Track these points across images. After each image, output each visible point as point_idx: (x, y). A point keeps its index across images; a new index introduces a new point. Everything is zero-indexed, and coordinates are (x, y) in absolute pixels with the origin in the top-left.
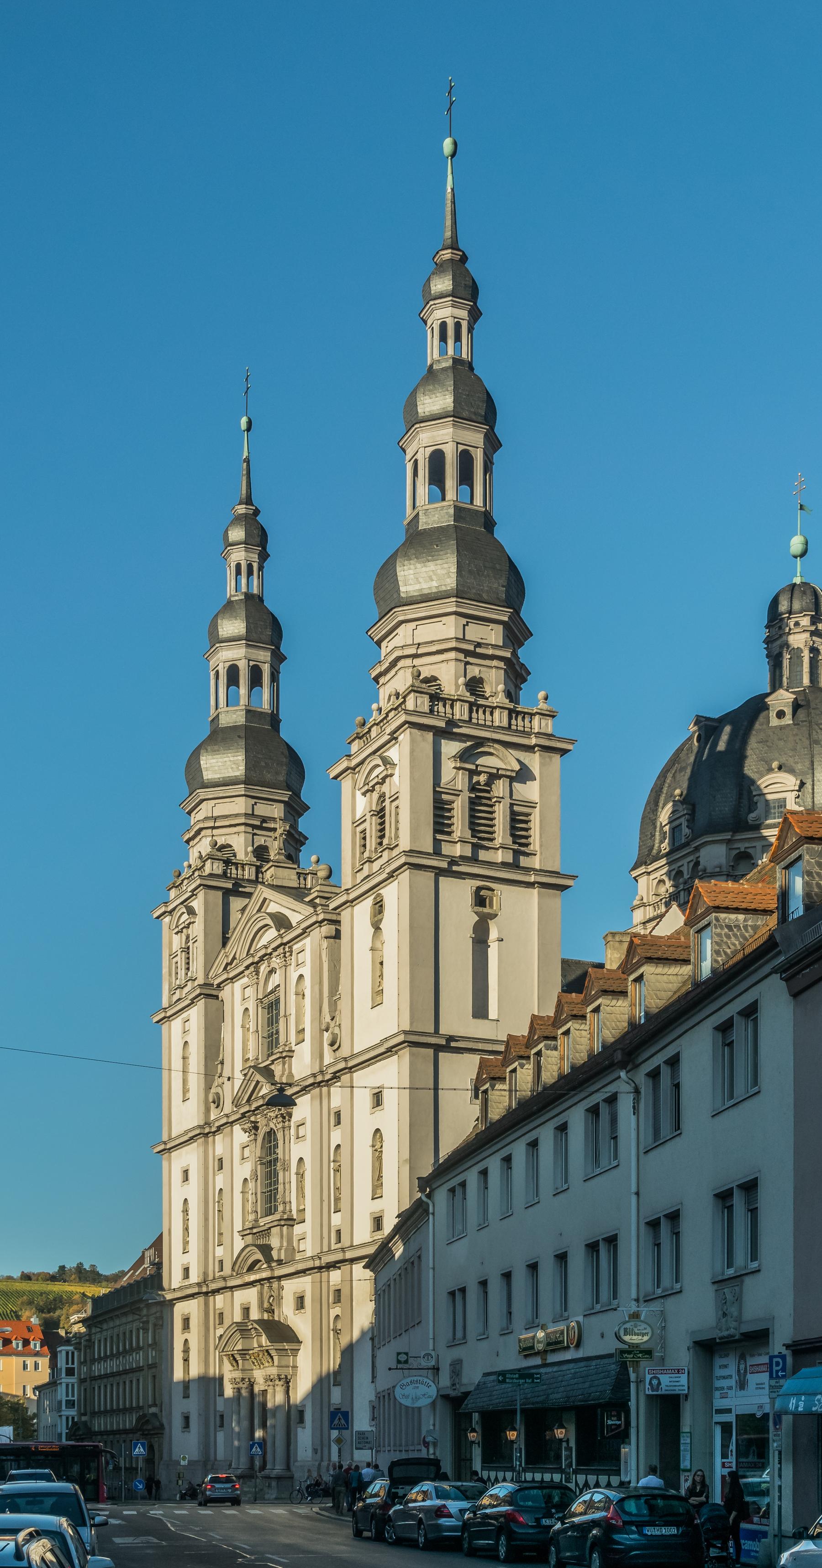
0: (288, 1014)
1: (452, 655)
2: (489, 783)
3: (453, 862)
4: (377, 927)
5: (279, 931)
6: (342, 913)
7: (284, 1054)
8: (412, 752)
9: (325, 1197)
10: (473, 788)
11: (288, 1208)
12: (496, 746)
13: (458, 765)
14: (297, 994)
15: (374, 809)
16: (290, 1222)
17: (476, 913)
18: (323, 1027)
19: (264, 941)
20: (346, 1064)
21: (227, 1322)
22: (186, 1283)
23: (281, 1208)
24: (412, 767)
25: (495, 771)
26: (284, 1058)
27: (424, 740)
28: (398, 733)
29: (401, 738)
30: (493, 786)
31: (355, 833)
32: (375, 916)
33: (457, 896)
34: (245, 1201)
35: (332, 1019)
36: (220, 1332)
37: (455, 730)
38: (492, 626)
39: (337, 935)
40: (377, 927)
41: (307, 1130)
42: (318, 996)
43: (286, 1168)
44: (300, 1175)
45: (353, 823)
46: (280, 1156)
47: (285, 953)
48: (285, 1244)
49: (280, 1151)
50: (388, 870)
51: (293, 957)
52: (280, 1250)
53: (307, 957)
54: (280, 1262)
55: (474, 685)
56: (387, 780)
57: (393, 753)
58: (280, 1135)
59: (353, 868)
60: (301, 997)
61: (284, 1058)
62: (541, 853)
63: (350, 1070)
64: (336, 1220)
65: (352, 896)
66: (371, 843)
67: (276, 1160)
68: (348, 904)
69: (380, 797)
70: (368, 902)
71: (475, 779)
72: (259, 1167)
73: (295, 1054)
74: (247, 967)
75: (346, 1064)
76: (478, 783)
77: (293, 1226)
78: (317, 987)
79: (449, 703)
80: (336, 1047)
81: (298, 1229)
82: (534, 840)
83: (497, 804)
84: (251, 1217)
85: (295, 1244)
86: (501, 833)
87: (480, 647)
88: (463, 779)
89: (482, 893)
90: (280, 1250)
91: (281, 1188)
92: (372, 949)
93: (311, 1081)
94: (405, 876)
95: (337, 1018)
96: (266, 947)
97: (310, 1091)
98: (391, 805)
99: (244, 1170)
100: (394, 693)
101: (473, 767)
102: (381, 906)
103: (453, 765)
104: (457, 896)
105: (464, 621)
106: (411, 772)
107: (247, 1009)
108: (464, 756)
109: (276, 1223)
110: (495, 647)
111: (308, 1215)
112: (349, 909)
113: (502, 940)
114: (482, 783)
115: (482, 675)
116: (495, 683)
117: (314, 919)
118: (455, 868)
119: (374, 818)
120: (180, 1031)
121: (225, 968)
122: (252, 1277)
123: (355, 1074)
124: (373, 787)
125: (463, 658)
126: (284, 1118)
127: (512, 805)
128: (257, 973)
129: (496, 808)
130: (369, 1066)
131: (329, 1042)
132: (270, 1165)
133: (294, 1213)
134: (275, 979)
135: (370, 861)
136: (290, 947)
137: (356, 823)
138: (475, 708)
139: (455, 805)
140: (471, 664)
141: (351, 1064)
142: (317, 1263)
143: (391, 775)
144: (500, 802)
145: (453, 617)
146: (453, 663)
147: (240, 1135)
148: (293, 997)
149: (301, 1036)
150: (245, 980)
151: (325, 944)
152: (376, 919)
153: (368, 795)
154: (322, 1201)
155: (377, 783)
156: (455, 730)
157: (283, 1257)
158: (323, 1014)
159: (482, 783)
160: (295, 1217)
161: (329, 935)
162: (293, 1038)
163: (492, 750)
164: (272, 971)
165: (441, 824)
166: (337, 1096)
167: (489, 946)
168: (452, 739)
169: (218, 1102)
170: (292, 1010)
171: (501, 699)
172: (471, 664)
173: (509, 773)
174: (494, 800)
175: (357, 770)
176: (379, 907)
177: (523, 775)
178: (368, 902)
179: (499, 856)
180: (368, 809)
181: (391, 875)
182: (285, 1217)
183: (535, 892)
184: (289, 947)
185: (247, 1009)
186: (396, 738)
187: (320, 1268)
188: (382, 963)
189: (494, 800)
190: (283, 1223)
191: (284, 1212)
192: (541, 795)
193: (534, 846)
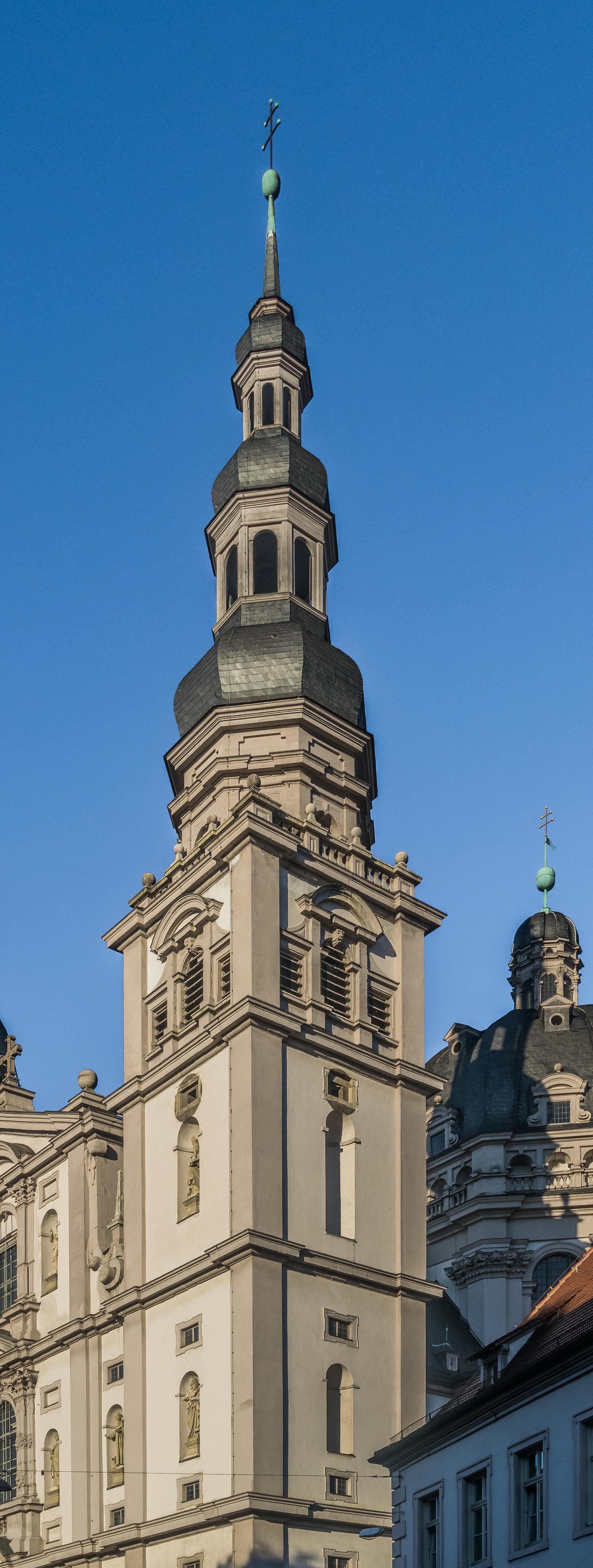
0: (29, 1261)
1: (297, 775)
2: (342, 946)
3: (306, 1028)
4: (188, 1120)
5: (19, 1157)
6: (125, 1115)
7: (26, 1307)
8: (254, 875)
10: (326, 944)
11: (31, 1492)
12: (355, 896)
13: (310, 909)
14: (43, 1236)
15: (179, 970)
16: (36, 1508)
17: (330, 1102)
18: (92, 1263)
20: (139, 1295)
23: (20, 1492)
24: (254, 895)
25: (352, 929)
26: (25, 1312)
27: (268, 865)
28: (229, 856)
29: (233, 863)
30: (347, 950)
31: (146, 1012)
32: (182, 1106)
33: (308, 1074)
35: (105, 1253)
37: (307, 862)
38: (342, 755)
39: (110, 1155)
40: (188, 1120)
42: (81, 1228)
43: (29, 1444)
44: (51, 1452)
45: (144, 999)
47: (26, 1187)
48: (29, 1534)
49: (19, 1427)
50: (214, 1033)
51: (38, 1193)
52: (22, 1540)
54: (23, 1555)
55: (324, 819)
56: (207, 928)
57: (219, 891)
58: (18, 1408)
59: (143, 1055)
60: (49, 1239)
61: (25, 1312)
62: (404, 1046)
63: (142, 1304)
65: (144, 1086)
66: (175, 1018)
67: (13, 1438)
68: (138, 1098)
69: (191, 955)
70: (172, 1091)
71: (327, 935)
73: (41, 1307)
75: (139, 1295)
76: (330, 941)
77: (39, 1512)
78: (80, 1218)
79: (295, 831)
80: (112, 1284)
82: (394, 1029)
83: (352, 974)
85: (42, 1534)
86: (357, 1011)
87: (332, 773)
88: (314, 930)
89: (336, 1079)
90: (22, 1540)
91: (20, 1467)
92: (178, 1149)
93: (76, 1328)
94: (245, 1038)
95: (115, 1251)
97: (68, 1346)
98: (212, 958)
100: (213, 819)
101: (328, 916)
102: (194, 1094)
103: (303, 908)
104: (308, 1074)
105: (310, 738)
106: (253, 901)
108: (315, 898)
109: (16, 1509)
110: (348, 776)
111: (66, 1497)
112: (139, 1106)
113: (360, 1143)
114: (334, 944)
115: (331, 813)
116: (345, 827)
117: (79, 1130)
118: (308, 1036)
119: (179, 985)
123: (147, 1312)
124: (181, 942)
125: (310, 783)
126: (25, 1383)
127: (370, 979)
129: (351, 979)
130: (175, 1294)
131: (103, 1278)
133: (41, 1498)
135: (175, 1037)
137: (147, 1000)
138: (325, 848)
139: (302, 962)
140: (319, 794)
141: (144, 1295)
142: (88, 1549)
143: (213, 919)
144: (356, 971)
145: (296, 730)
146: (296, 787)
148: (37, 1240)
149: (51, 1285)
151: (93, 1162)
152: (185, 1109)
153: (170, 957)
155: (190, 934)
156: (307, 862)
157: (27, 1548)
158: (89, 1249)
159: (334, 944)
160: (42, 1501)
161: (99, 1150)
162: (37, 1288)
163: (349, 901)
165: (289, 979)
166: (113, 1345)
167: (342, 1150)
168: (300, 876)
170: (37, 1256)
171: (355, 843)
172: (319, 794)
173: (368, 936)
174: (347, 969)
175: (150, 930)
176: (191, 1093)
177: (379, 946)
178: (172, 1091)
179: (357, 1037)
180: (171, 973)
181: (220, 1042)
182: (29, 1501)
183: (397, 1092)
184: (32, 1179)
186: (226, 865)
187: (89, 1557)
188: (195, 1164)
189: (347, 969)
190: (26, 1508)
191: (26, 1497)
192: (404, 974)
193: (394, 1035)
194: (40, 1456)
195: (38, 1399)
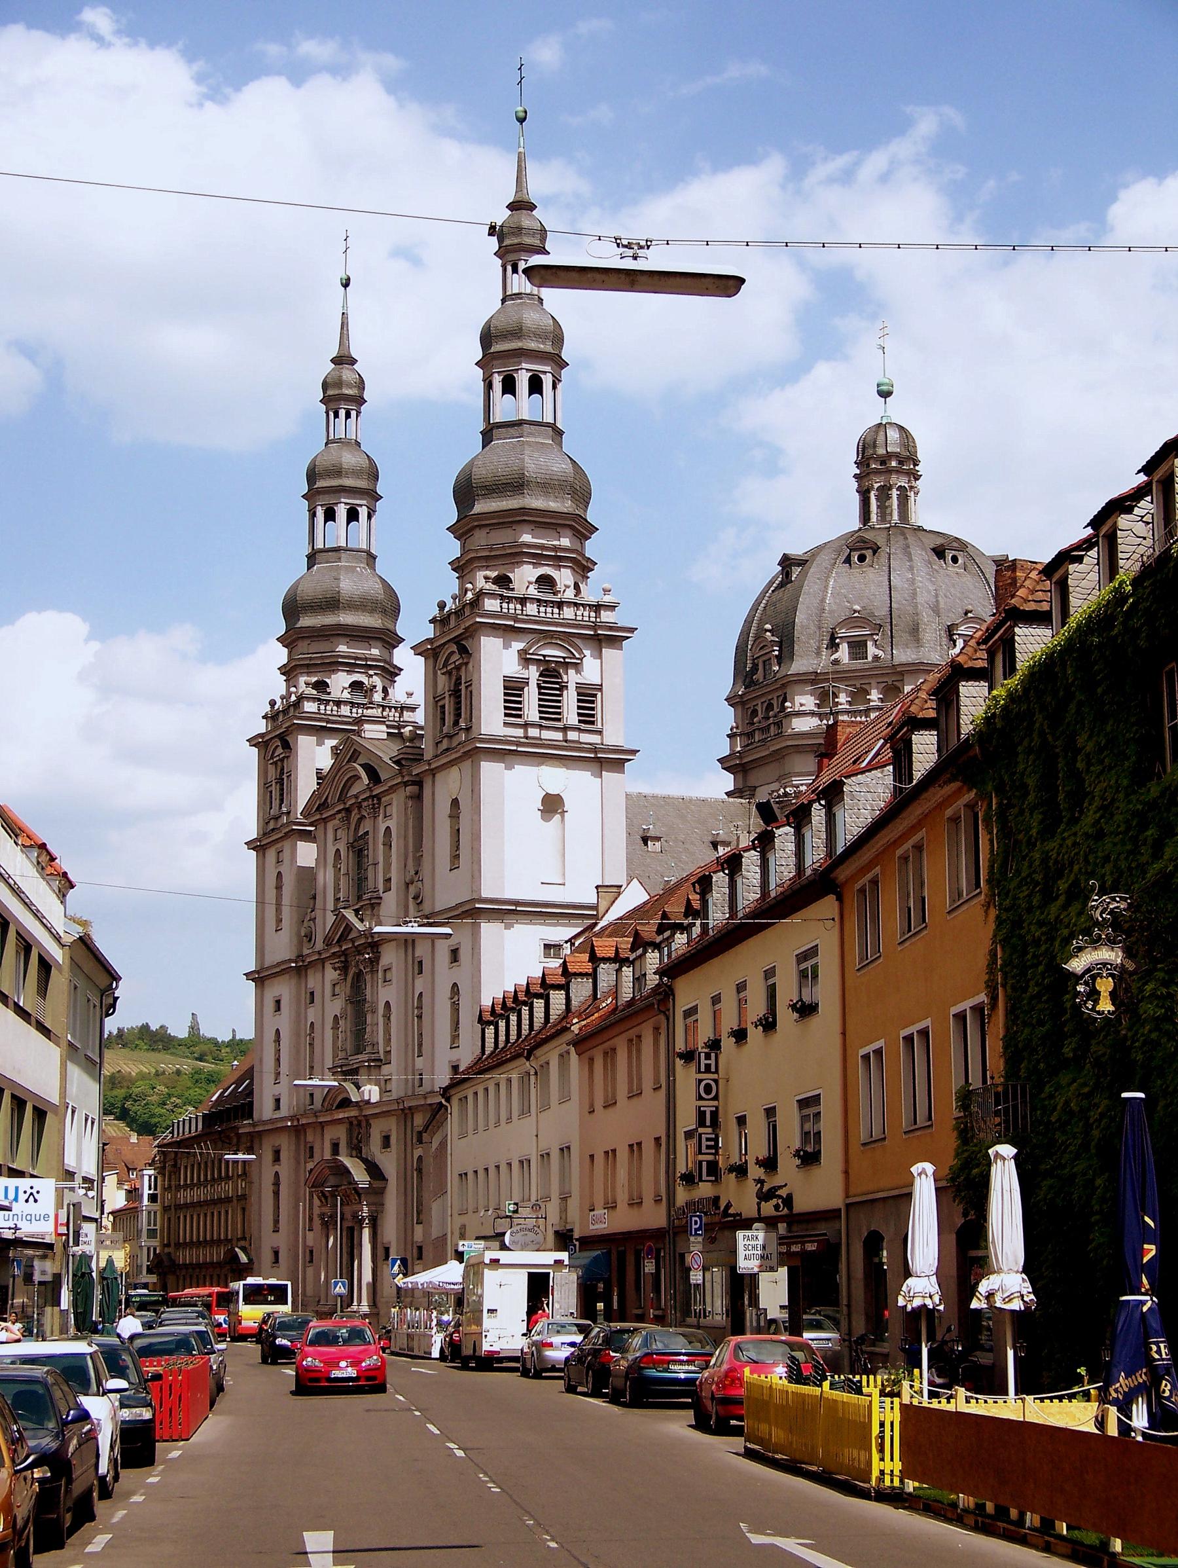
9: (410, 1039)
19: (354, 791)
21: (317, 1158)
22: (277, 1115)
34: (335, 1038)
36: (310, 1166)
41: (394, 975)
43: (374, 1012)
44: (387, 1017)
46: (368, 997)
49: (368, 992)
53: (394, 810)
58: (368, 977)
64: (419, 1063)
72: (349, 1007)
74: (339, 812)
81: (385, 1069)
84: (341, 1055)
96: (356, 796)
99: (335, 1007)
107: (338, 850)
120: (274, 860)
121: (317, 809)
122: (341, 1116)
128: (348, 819)
132: (358, 1004)
134: (367, 826)
136: (379, 799)
147: (331, 974)
150: (336, 822)
154: (407, 1045)
164: (363, 818)
169: (309, 937)
185: (338, 850)
194: (381, 1020)
195: (380, 974)
